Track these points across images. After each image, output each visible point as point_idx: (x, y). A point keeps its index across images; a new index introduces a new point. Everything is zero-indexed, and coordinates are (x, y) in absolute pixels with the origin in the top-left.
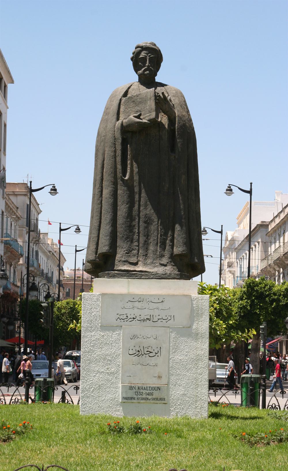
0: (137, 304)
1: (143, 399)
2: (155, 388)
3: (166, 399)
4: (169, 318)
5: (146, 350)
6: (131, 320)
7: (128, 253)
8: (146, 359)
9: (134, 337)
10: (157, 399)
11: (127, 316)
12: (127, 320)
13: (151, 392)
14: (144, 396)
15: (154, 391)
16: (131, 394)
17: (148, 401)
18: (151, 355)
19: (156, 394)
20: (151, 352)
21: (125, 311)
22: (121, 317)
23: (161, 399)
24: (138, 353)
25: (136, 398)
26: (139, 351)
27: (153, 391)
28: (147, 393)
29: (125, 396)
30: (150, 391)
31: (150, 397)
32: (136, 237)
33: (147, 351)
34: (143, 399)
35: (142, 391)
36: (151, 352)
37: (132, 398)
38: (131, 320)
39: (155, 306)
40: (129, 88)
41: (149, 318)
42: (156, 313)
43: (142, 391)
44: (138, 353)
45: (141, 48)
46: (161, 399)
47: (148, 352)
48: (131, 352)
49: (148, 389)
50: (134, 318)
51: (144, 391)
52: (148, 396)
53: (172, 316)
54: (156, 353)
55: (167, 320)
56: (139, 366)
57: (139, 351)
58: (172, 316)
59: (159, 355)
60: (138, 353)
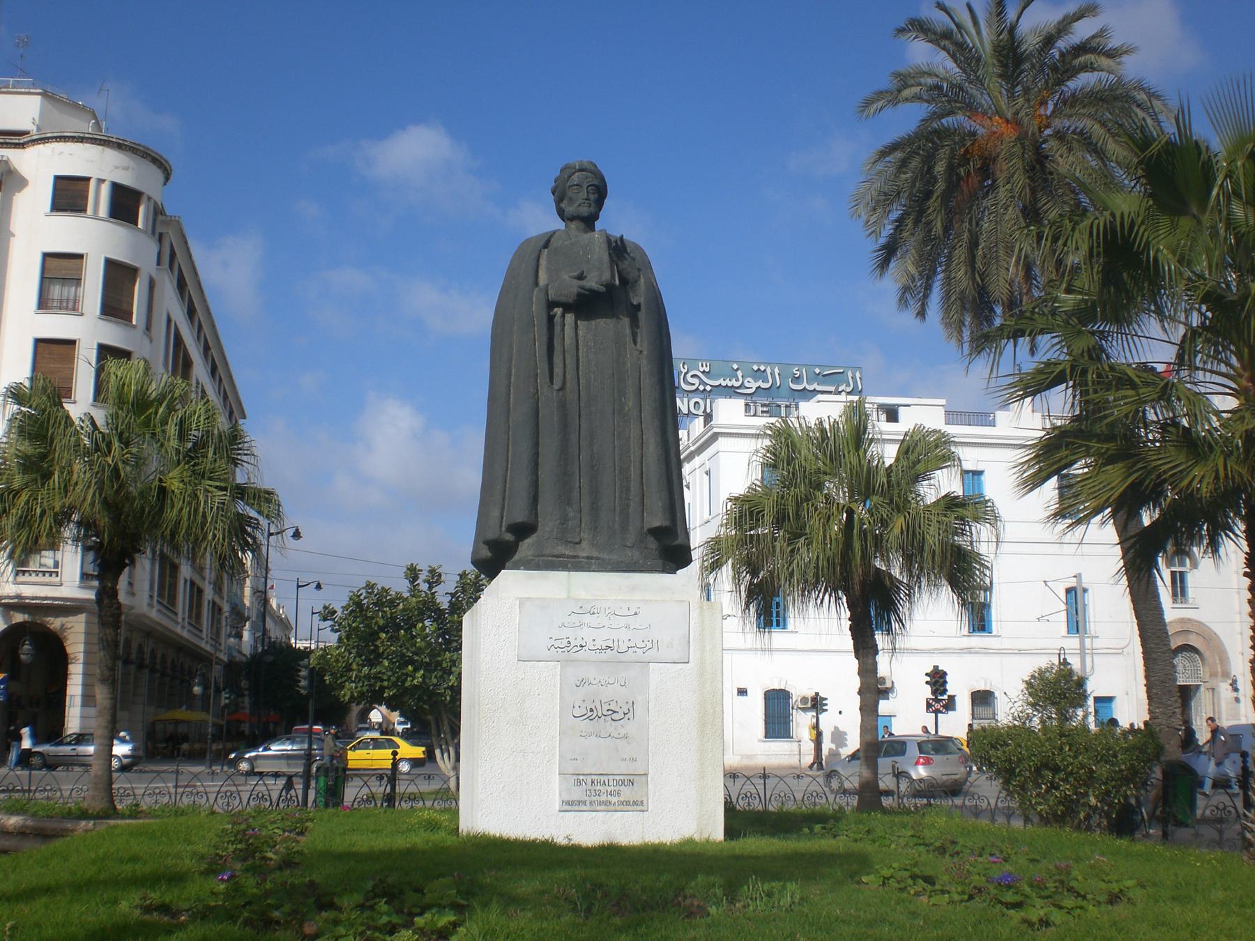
0: (587, 619)
1: (601, 803)
2: (623, 782)
3: (645, 803)
4: (649, 645)
5: (606, 707)
6: (576, 649)
7: (563, 524)
8: (607, 726)
9: (583, 682)
10: (628, 803)
11: (569, 643)
12: (569, 649)
13: (617, 788)
14: (604, 798)
15: (622, 788)
16: (578, 794)
17: (611, 807)
18: (615, 716)
19: (627, 794)
20: (615, 712)
21: (566, 632)
22: (557, 644)
23: (635, 803)
24: (592, 714)
25: (588, 803)
26: (592, 710)
27: (621, 788)
28: (609, 791)
29: (566, 798)
30: (615, 788)
31: (614, 799)
32: (575, 494)
33: (608, 710)
34: (601, 803)
35: (599, 787)
36: (615, 712)
37: (579, 802)
38: (576, 649)
39: (623, 621)
40: (551, 236)
41: (612, 645)
42: (623, 635)
43: (599, 787)
44: (590, 714)
45: (568, 171)
46: (635, 803)
47: (611, 712)
48: (577, 713)
49: (611, 783)
50: (582, 646)
51: (603, 789)
52: (610, 798)
53: (655, 642)
54: (625, 714)
55: (645, 649)
56: (593, 738)
57: (592, 710)
58: (655, 642)
59: (631, 718)
60: (590, 714)
